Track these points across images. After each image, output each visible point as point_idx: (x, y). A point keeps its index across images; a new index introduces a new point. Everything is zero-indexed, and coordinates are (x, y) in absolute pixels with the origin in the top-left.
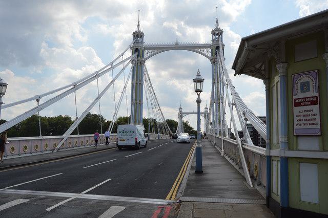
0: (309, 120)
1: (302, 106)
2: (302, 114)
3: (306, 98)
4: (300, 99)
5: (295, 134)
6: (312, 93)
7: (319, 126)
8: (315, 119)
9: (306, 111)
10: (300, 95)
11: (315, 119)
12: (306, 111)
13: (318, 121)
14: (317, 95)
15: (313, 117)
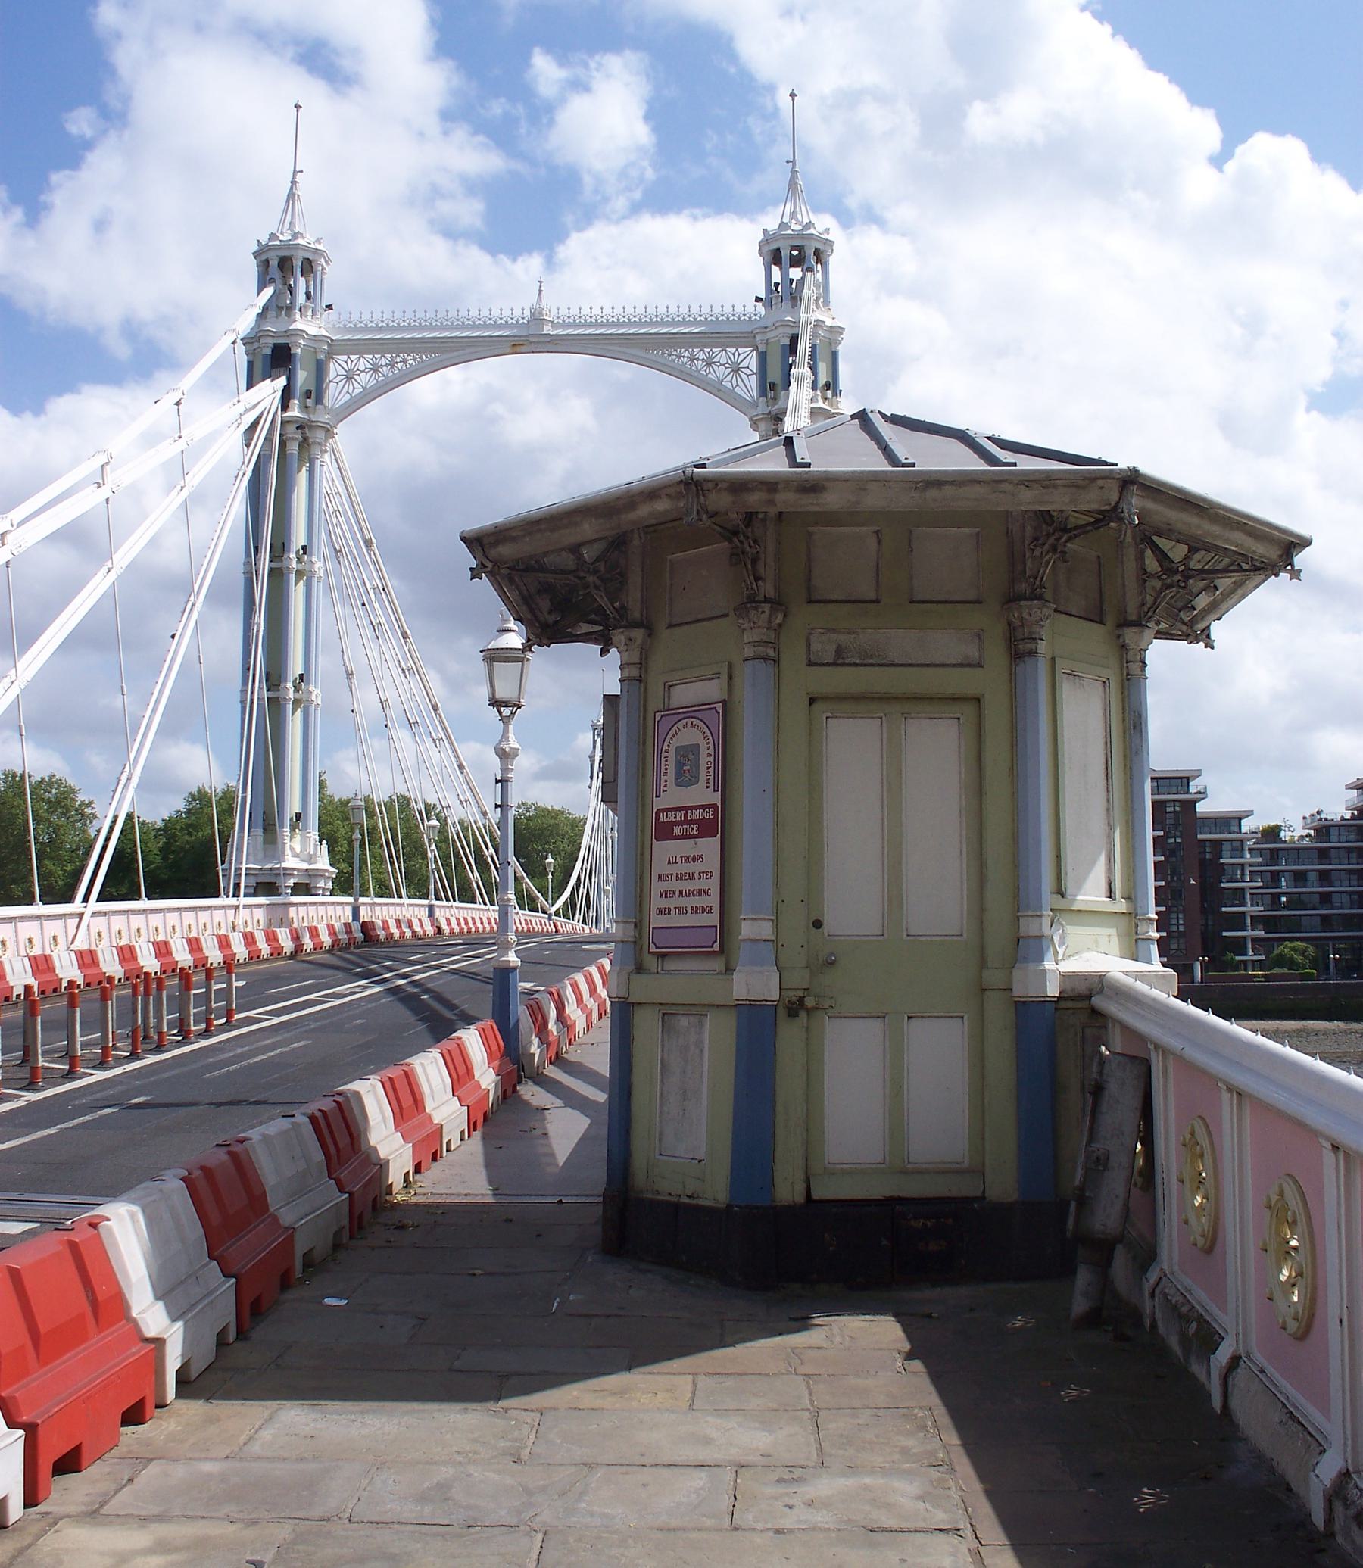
0: (691, 894)
1: (678, 838)
2: (675, 869)
3: (686, 809)
4: (671, 810)
5: (653, 949)
6: (703, 794)
7: (714, 919)
8: (707, 893)
9: (687, 859)
10: (673, 796)
11: (707, 893)
12: (687, 859)
13: (714, 900)
14: (716, 798)
15: (703, 884)
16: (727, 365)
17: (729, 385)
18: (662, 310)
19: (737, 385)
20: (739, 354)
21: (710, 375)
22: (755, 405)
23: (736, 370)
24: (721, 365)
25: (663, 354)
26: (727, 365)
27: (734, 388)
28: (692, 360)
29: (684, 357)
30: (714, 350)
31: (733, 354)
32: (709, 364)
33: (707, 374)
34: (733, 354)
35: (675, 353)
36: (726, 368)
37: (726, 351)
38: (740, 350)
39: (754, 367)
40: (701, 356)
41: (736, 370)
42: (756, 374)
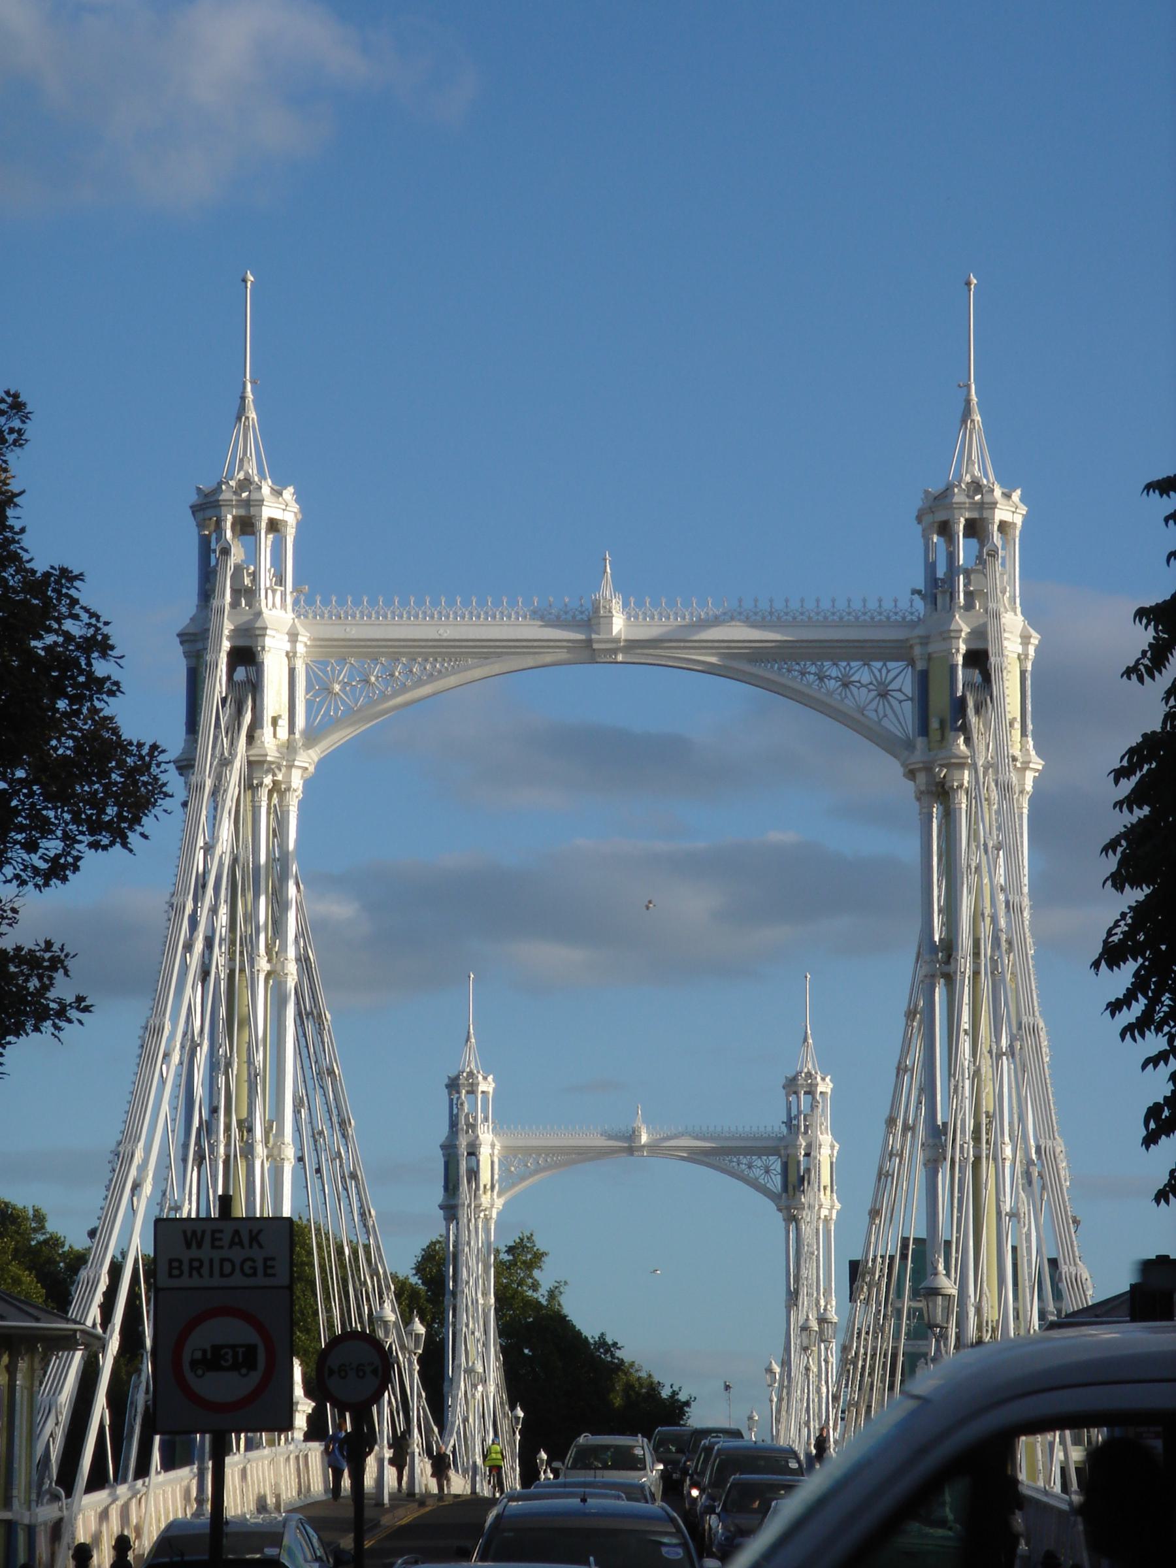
16: (871, 687)
17: (873, 715)
18: (779, 605)
19: (885, 716)
20: (888, 671)
21: (846, 701)
22: (909, 746)
23: (884, 695)
24: (863, 686)
25: (780, 669)
26: (871, 687)
27: (880, 720)
28: (821, 679)
29: (809, 673)
30: (853, 664)
31: (880, 671)
32: (846, 685)
33: (842, 700)
34: (880, 671)
35: (797, 667)
36: (869, 691)
37: (868, 665)
38: (891, 665)
39: (908, 689)
40: (834, 672)
41: (884, 695)
42: (911, 699)
